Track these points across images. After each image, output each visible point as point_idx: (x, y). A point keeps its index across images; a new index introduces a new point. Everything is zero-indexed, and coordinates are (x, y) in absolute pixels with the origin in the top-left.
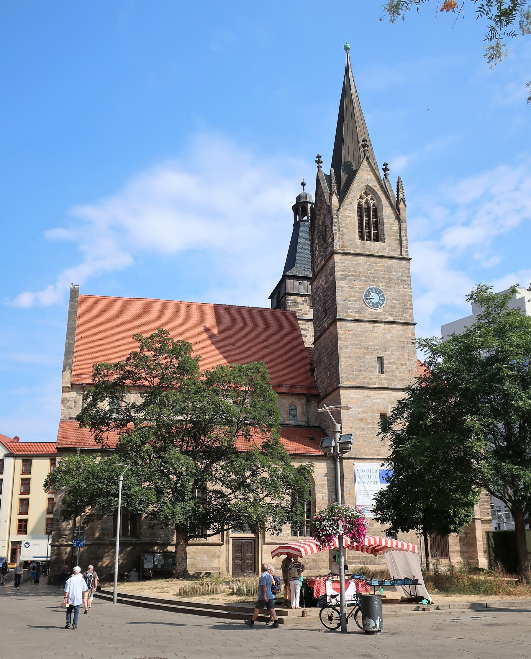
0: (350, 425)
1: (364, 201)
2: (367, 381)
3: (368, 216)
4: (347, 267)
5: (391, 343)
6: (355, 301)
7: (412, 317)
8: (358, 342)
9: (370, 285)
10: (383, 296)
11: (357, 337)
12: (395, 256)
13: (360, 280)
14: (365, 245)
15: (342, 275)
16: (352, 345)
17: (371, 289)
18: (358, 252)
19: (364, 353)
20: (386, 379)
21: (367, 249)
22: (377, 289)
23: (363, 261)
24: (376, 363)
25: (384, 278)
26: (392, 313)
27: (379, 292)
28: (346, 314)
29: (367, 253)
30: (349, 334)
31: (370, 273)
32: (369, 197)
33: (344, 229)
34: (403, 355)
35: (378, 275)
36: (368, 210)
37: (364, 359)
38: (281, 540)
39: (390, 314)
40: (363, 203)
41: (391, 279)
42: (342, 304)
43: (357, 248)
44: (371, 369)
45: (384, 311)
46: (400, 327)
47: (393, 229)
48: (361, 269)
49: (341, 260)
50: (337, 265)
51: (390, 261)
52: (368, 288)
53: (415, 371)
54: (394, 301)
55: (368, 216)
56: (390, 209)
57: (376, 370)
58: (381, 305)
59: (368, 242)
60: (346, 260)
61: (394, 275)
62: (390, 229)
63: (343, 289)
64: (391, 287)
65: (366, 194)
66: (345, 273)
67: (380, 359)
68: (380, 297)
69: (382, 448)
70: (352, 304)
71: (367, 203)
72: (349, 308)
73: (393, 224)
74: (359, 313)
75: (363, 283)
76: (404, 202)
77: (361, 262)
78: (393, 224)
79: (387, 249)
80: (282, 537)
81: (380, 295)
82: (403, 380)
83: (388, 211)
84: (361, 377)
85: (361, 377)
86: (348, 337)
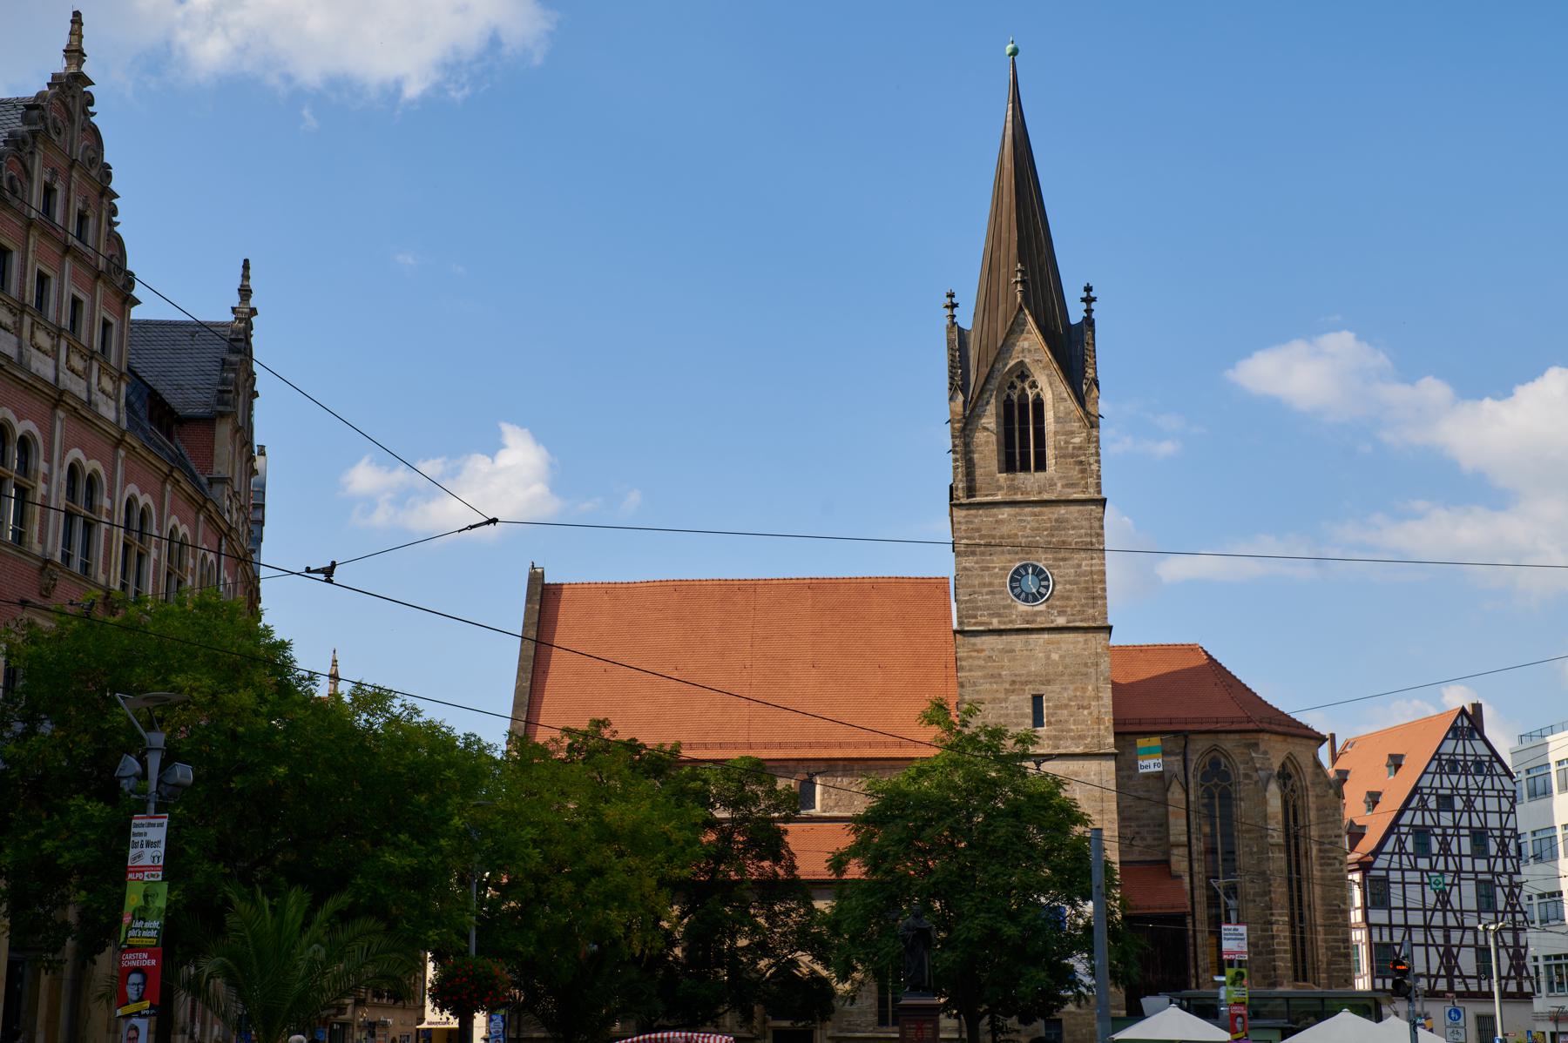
1: (1017, 392)
4: (978, 530)
5: (1060, 668)
6: (992, 593)
7: (1104, 615)
8: (996, 672)
9: (1020, 560)
11: (994, 661)
12: (1076, 496)
13: (1003, 552)
14: (1016, 482)
16: (984, 677)
17: (1025, 567)
18: (999, 498)
20: (1049, 738)
21: (1018, 488)
22: (1035, 568)
23: (1009, 515)
26: (1064, 609)
27: (1039, 573)
28: (973, 621)
29: (1019, 497)
30: (980, 658)
31: (1023, 536)
34: (1084, 689)
35: (1038, 538)
37: (1006, 702)
38: (857, 1031)
40: (1015, 397)
42: (966, 602)
43: (1000, 488)
44: (1020, 720)
45: (1048, 607)
47: (1071, 443)
48: (1005, 530)
49: (965, 517)
50: (959, 526)
51: (1063, 510)
52: (1018, 565)
53: (1106, 718)
54: (1068, 587)
59: (1021, 475)
60: (976, 516)
61: (1072, 536)
62: (1067, 442)
63: (969, 573)
64: (1064, 559)
66: (973, 542)
67: (1037, 700)
68: (1040, 581)
70: (986, 601)
72: (978, 608)
74: (999, 615)
75: (1009, 557)
76: (1097, 386)
77: (1005, 516)
79: (1059, 485)
80: (858, 1028)
81: (1041, 577)
83: (1062, 408)
86: (976, 662)
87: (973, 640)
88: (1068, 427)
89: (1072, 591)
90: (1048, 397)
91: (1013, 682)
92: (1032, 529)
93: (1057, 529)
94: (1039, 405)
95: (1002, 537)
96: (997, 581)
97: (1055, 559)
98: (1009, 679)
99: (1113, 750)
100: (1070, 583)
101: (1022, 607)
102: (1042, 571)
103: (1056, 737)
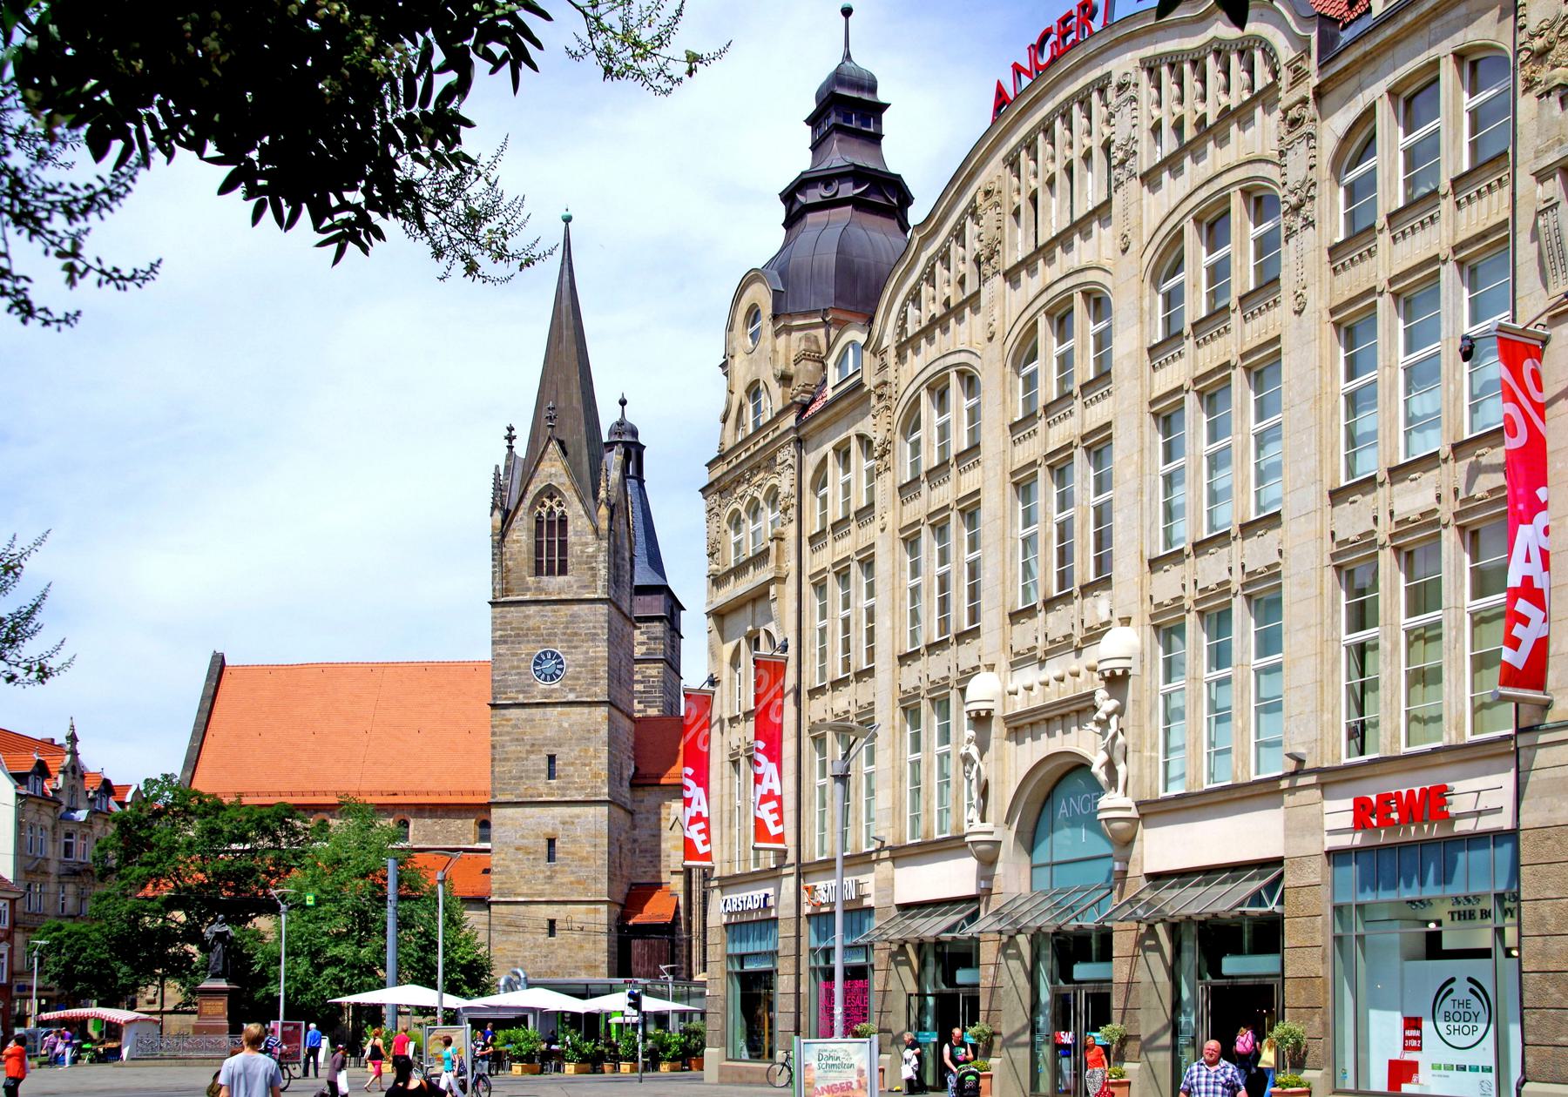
0: (503, 856)
2: (530, 792)
3: (551, 533)
4: (510, 623)
6: (519, 674)
10: (562, 663)
15: (501, 636)
16: (511, 741)
17: (545, 653)
18: (527, 597)
19: (528, 752)
20: (558, 788)
24: (544, 765)
25: (564, 634)
29: (543, 597)
32: (554, 504)
33: (510, 563)
34: (586, 751)
36: (551, 524)
39: (572, 690)
40: (544, 515)
41: (576, 634)
43: (528, 589)
46: (586, 710)
48: (531, 623)
51: (576, 608)
55: (551, 533)
56: (585, 519)
57: (544, 775)
58: (558, 676)
59: (545, 578)
61: (583, 628)
62: (582, 552)
64: (575, 647)
65: (551, 498)
69: (547, 886)
71: (551, 512)
72: (510, 686)
73: (586, 544)
74: (524, 692)
75: (533, 645)
78: (586, 544)
82: (582, 788)
84: (522, 788)
85: (522, 788)
86: (506, 729)
87: (503, 712)
88: (584, 540)
89: (580, 672)
90: (569, 513)
91: (533, 745)
92: (552, 623)
93: (574, 623)
94: (563, 521)
95: (528, 629)
96: (523, 665)
97: (569, 647)
98: (531, 742)
99: (607, 798)
100: (580, 666)
101: (543, 685)
102: (558, 657)
103: (563, 788)
